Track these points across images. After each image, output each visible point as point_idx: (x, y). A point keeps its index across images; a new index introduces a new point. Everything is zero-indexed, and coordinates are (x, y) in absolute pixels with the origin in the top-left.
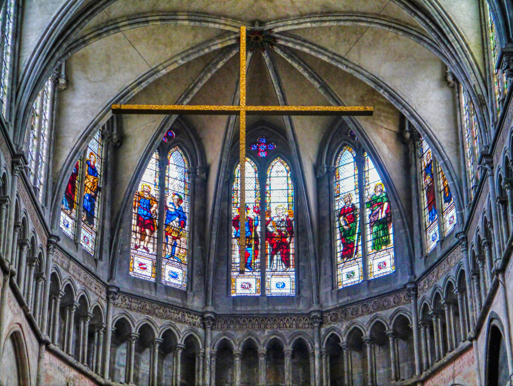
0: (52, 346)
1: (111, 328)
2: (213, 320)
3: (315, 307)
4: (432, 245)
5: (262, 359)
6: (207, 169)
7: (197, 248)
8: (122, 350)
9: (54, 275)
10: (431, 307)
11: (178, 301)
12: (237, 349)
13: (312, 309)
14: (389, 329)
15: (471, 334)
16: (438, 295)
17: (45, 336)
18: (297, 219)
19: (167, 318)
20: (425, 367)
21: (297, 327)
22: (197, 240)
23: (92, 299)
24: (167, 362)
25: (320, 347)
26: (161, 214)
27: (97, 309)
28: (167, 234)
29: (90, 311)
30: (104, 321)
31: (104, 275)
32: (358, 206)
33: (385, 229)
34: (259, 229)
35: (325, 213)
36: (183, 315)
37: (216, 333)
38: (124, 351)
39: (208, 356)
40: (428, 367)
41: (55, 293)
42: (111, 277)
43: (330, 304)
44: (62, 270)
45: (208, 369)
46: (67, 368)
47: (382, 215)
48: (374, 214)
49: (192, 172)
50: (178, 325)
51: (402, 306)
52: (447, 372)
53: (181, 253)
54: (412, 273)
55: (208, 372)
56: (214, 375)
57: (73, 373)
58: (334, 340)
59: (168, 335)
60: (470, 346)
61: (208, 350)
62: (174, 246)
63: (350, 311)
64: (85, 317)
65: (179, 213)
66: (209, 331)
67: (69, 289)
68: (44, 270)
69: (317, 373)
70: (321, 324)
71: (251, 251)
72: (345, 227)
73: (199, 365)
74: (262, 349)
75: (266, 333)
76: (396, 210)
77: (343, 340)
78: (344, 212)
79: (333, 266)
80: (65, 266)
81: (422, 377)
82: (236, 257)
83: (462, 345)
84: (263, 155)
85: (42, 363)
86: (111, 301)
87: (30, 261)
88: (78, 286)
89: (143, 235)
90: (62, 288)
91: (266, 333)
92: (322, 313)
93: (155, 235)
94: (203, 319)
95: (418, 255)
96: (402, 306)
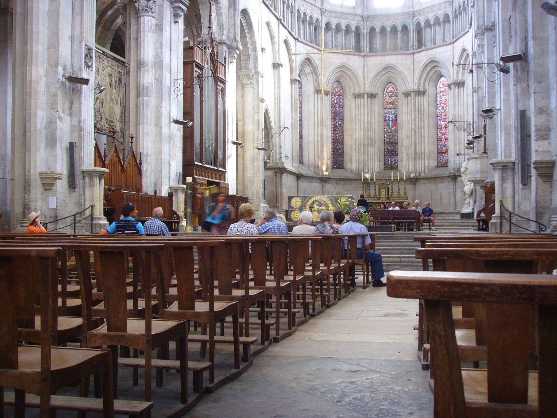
0: (300, 40)
1: (324, 26)
2: (367, 18)
3: (411, 10)
5: (388, 34)
8: (329, 34)
9: (298, 10)
10: (458, 11)
12: (378, 30)
13: (409, 11)
14: (441, 19)
15: (469, 26)
16: (460, 6)
17: (296, 37)
19: (347, 19)
20: (455, 36)
21: (403, 19)
23: (314, 16)
24: (348, 37)
25: (413, 27)
27: (317, 19)
30: (320, 24)
31: (319, 5)
36: (354, 17)
37: (368, 23)
38: (330, 34)
39: (365, 34)
40: (456, 36)
41: (299, 17)
42: (322, 5)
44: (301, 7)
45: (366, 39)
46: (307, 47)
50: (352, 22)
51: (447, 9)
52: (462, 39)
55: (365, 41)
56: (368, 42)
57: (310, 48)
58: (419, 24)
59: (348, 27)
60: (469, 31)
61: (365, 31)
63: (425, 11)
64: (313, 24)
66: (365, 22)
67: (305, 14)
68: (294, 10)
69: (411, 38)
70: (414, 17)
73: (362, 38)
75: (390, 22)
77: (423, 24)
80: (302, 5)
81: (453, 41)
83: (467, 30)
85: (297, 47)
86: (323, 15)
87: (288, 8)
90: (302, 15)
91: (390, 22)
92: (414, 12)
94: (363, 18)
96: (447, 9)
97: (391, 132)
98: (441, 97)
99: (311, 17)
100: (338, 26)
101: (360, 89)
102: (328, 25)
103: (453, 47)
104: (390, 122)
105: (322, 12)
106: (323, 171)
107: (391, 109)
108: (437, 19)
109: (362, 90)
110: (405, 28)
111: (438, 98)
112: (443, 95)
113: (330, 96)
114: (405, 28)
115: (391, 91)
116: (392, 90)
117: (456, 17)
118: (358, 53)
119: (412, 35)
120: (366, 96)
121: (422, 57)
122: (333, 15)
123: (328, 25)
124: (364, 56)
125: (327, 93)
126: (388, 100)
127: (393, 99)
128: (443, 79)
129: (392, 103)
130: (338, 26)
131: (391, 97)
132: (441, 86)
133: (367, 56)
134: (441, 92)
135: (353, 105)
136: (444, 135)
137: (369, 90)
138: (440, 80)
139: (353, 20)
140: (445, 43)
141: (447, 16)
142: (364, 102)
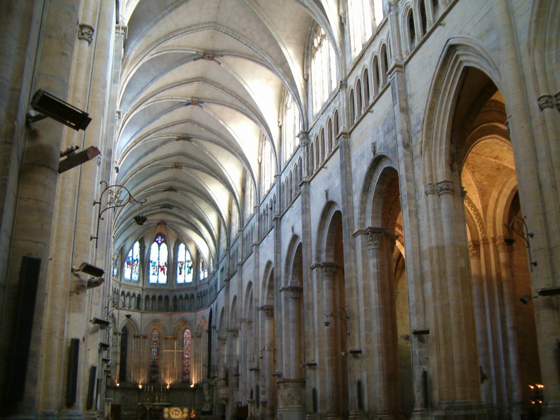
1: (120, 293)
4: (202, 278)
6: (144, 247)
7: (141, 269)
11: (136, 285)
12: (151, 297)
18: (168, 261)
22: (141, 268)
26: (132, 261)
27: (118, 290)
28: (134, 266)
29: (116, 291)
31: (119, 280)
32: (184, 261)
33: (191, 269)
34: (157, 265)
35: (175, 261)
42: (121, 280)
43: (175, 288)
47: (190, 265)
48: (188, 265)
49: (140, 247)
50: (136, 291)
52: (202, 311)
53: (137, 271)
54: (196, 284)
58: (175, 297)
59: (134, 295)
62: (135, 269)
65: (137, 260)
71: (155, 270)
72: (181, 266)
74: (157, 298)
76: (194, 267)
77: (178, 297)
78: (180, 262)
79: (176, 277)
82: (151, 272)
84: (160, 242)
88: (114, 286)
89: (128, 267)
93: (131, 266)
95: (198, 280)
97: (155, 359)
98: (186, 341)
99: (115, 289)
100: (129, 294)
101: (138, 332)
102: (123, 293)
103: (196, 315)
104: (155, 353)
105: (120, 286)
106: (115, 384)
107: (155, 345)
108: (187, 296)
109: (140, 333)
110: (167, 297)
111: (185, 341)
112: (187, 340)
113: (121, 336)
114: (167, 297)
115: (155, 334)
116: (156, 334)
117: (198, 297)
118: (138, 311)
119: (171, 303)
120: (142, 337)
121: (177, 316)
122: (126, 287)
123: (123, 293)
124: (142, 313)
125: (120, 335)
126: (154, 339)
127: (156, 339)
128: (188, 330)
129: (156, 341)
130: (129, 294)
131: (155, 338)
132: (186, 334)
133: (144, 313)
134: (186, 338)
135: (133, 342)
136: (187, 363)
137: (143, 333)
138: (186, 331)
139: (137, 290)
140: (190, 310)
141: (193, 296)
142: (140, 341)
